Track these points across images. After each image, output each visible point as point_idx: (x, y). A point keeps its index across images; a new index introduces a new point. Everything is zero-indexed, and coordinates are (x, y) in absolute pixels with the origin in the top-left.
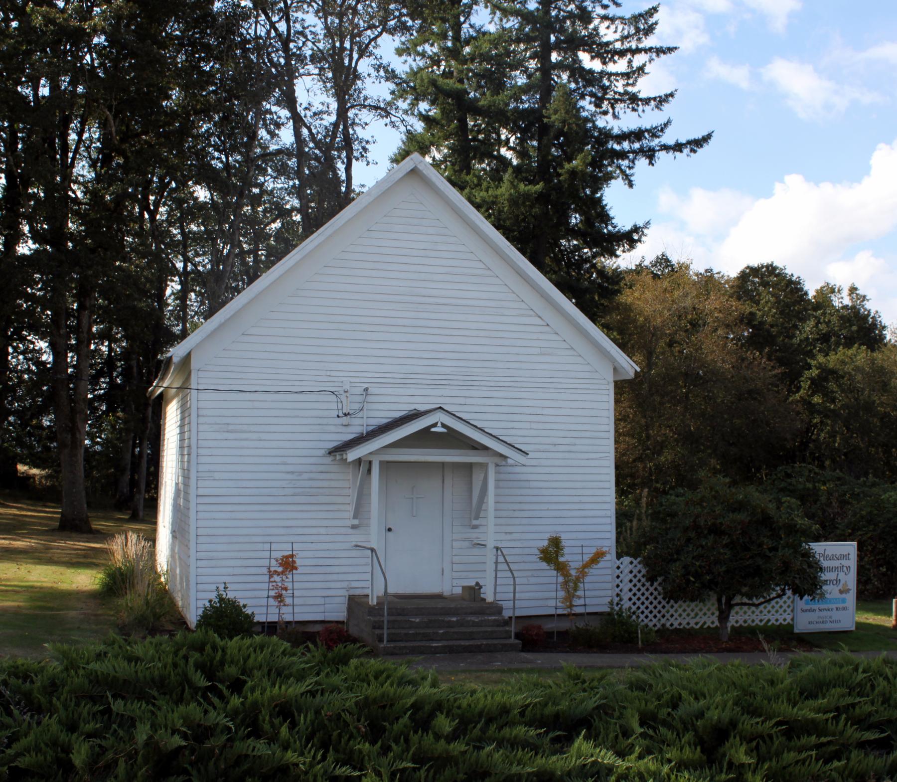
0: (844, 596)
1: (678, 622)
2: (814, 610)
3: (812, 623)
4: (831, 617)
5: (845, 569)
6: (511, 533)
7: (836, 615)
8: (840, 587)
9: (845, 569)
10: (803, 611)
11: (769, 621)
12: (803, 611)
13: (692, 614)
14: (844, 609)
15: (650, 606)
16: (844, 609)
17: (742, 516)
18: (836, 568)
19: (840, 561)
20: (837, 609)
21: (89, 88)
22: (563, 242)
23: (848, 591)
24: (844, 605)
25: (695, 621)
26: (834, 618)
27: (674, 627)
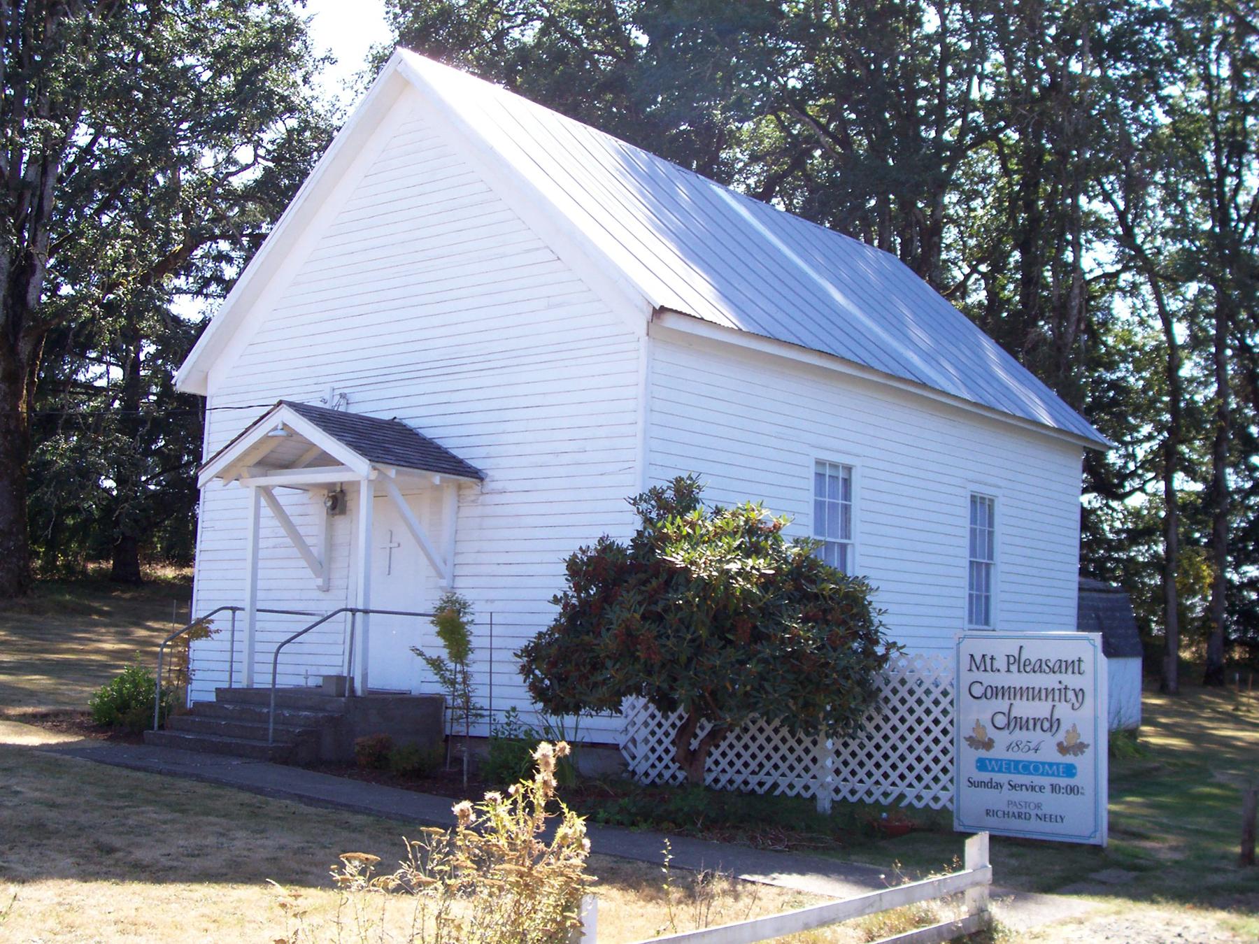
0: (1069, 759)
1: (849, 786)
2: (999, 786)
3: (995, 813)
4: (1038, 806)
5: (1071, 695)
6: (493, 601)
7: (1051, 803)
8: (1061, 736)
9: (1071, 695)
10: (972, 783)
11: (902, 796)
12: (972, 783)
13: (753, 765)
14: (1072, 790)
15: (899, 763)
16: (1072, 790)
17: (760, 564)
18: (1049, 692)
19: (1058, 677)
20: (1054, 788)
21: (1152, 421)
22: (1095, 319)
23: (1080, 748)
24: (1072, 782)
25: (756, 779)
26: (1046, 809)
27: (750, 787)
